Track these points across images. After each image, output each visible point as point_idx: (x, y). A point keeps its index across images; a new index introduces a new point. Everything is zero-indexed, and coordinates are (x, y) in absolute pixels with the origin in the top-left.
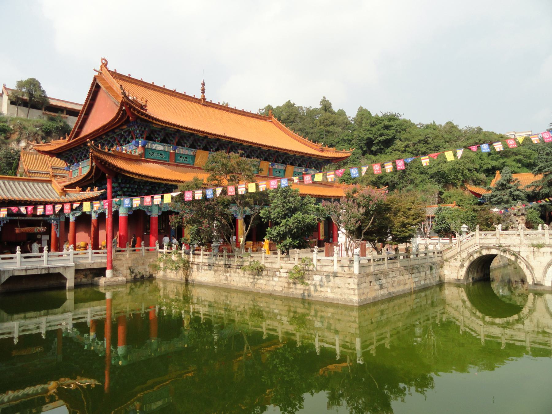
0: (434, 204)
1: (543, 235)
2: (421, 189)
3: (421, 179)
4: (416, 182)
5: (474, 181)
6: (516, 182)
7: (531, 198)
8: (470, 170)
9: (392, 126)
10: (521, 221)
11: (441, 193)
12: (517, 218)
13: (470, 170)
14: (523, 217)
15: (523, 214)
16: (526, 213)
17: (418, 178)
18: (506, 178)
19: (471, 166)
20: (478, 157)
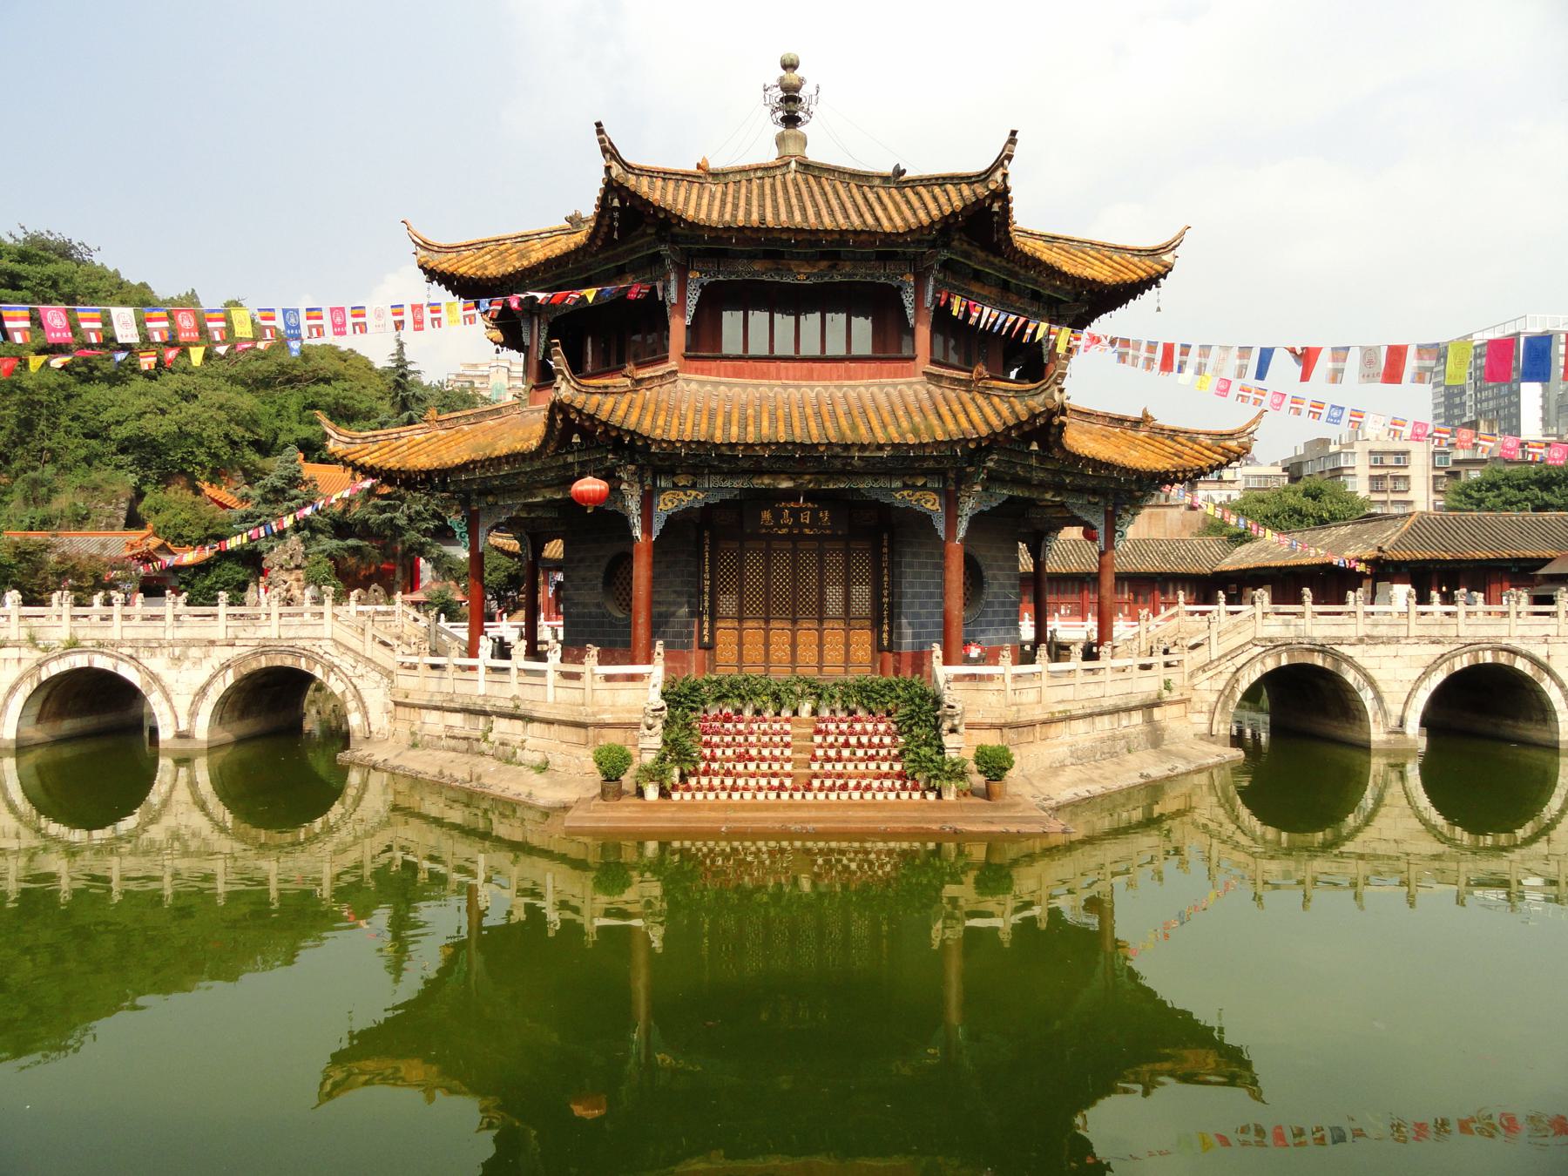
0: (110, 527)
1: (59, 616)
2: (77, 482)
3: (83, 452)
4: (68, 459)
5: (246, 473)
6: (311, 486)
7: (341, 527)
8: (234, 444)
9: (27, 278)
10: (295, 584)
11: (139, 495)
12: (285, 576)
13: (234, 444)
14: (300, 574)
15: (298, 567)
16: (305, 564)
17: (77, 448)
18: (285, 473)
19: (238, 432)
20: (273, 411)
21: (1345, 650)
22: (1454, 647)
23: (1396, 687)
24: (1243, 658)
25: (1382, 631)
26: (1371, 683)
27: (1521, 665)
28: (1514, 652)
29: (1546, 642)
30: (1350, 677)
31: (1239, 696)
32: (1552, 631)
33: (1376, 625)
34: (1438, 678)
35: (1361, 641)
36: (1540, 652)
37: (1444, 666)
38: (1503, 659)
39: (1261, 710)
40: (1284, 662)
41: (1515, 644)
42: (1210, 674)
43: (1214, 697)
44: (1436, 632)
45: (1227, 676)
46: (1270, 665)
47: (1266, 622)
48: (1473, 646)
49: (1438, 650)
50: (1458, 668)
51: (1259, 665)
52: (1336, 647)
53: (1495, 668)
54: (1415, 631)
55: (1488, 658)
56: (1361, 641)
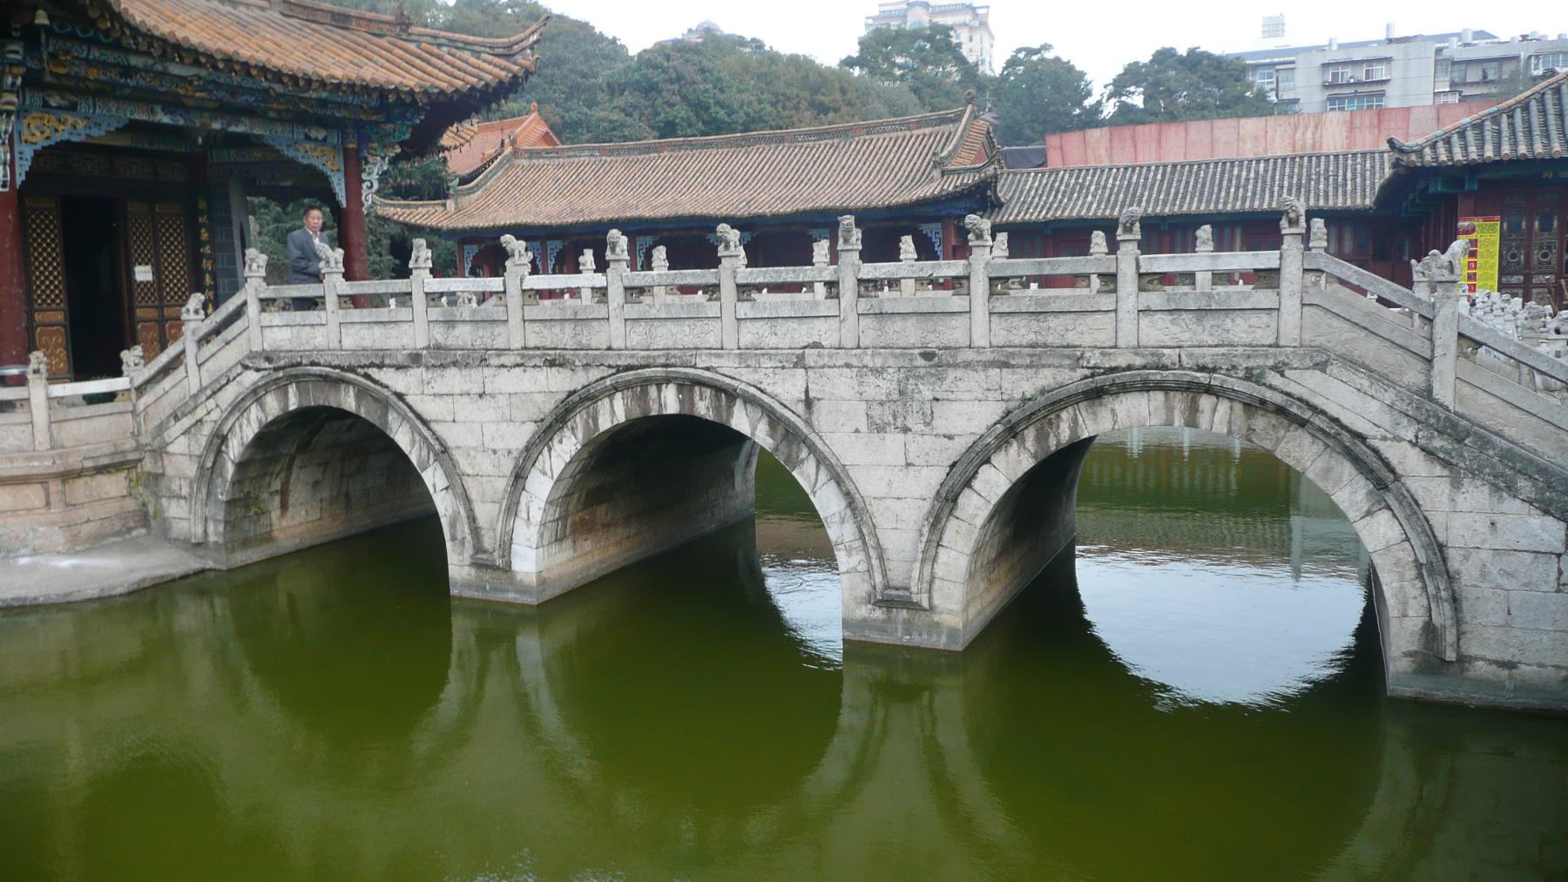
21: (394, 380)
22: (595, 374)
23: (485, 464)
24: (229, 395)
25: (463, 336)
26: (443, 453)
27: (740, 421)
28: (726, 394)
29: (800, 363)
30: (402, 437)
31: (230, 470)
32: (824, 332)
33: (450, 323)
34: (566, 448)
35: (415, 359)
36: (787, 389)
37: (579, 420)
38: (703, 407)
39: (243, 505)
40: (293, 404)
41: (728, 369)
42: (186, 422)
43: (191, 470)
44: (564, 337)
45: (207, 429)
46: (273, 406)
47: (267, 318)
48: (634, 378)
49: (561, 382)
50: (605, 424)
51: (254, 409)
52: (373, 372)
53: (686, 423)
54: (513, 335)
55: (670, 402)
56: (415, 359)
